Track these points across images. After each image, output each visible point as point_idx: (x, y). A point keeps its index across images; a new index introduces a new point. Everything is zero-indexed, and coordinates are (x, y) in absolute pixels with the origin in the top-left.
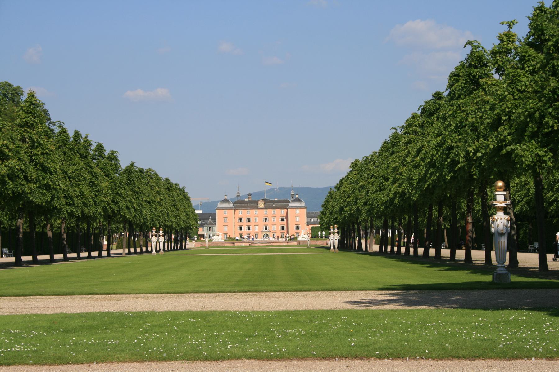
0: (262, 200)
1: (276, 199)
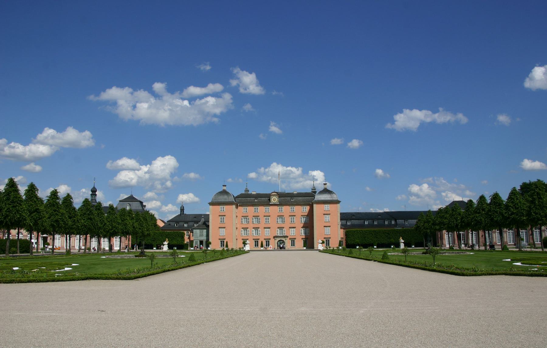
1: (295, 193)
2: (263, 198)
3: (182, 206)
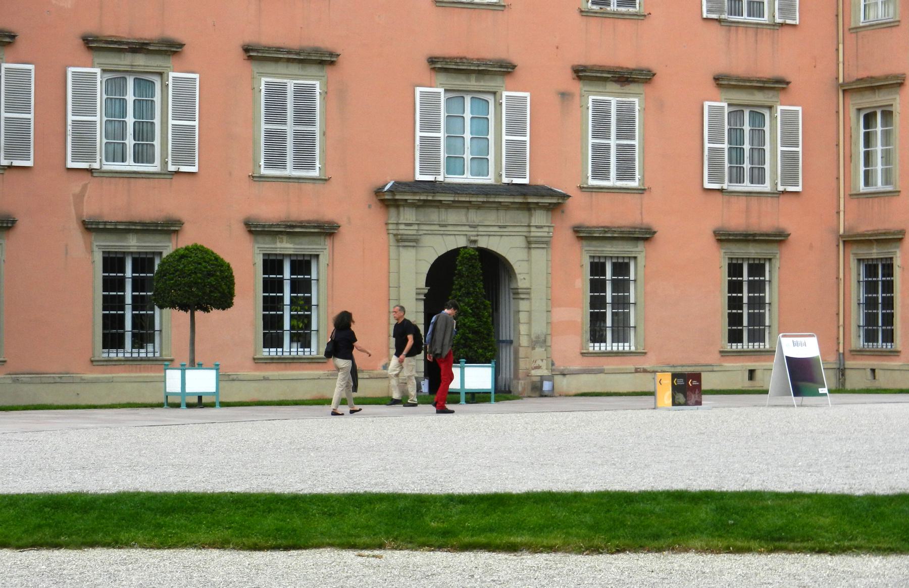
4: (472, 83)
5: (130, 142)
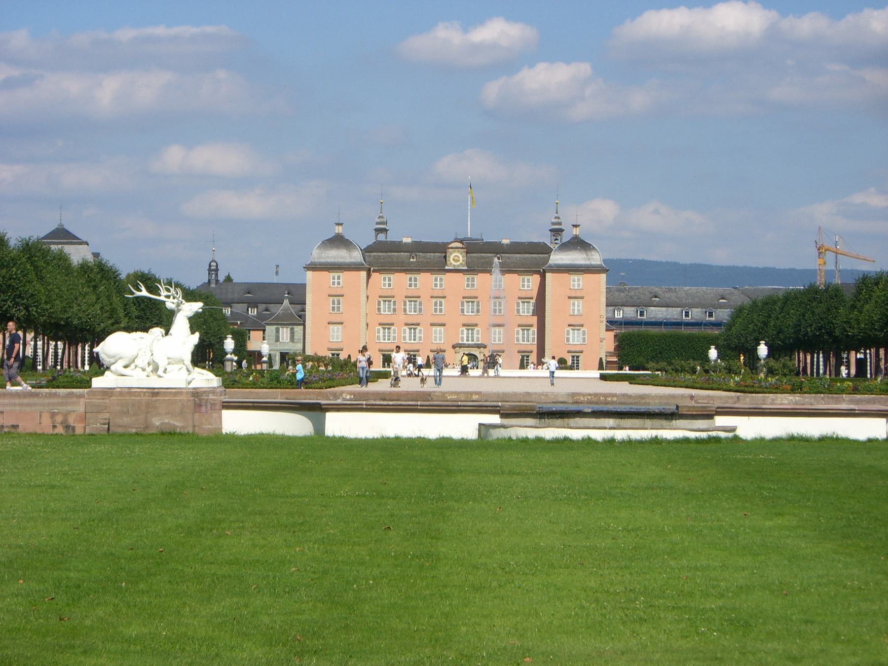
0: (461, 241)
1: (506, 241)
2: (429, 254)
3: (214, 261)
4: (470, 327)
5: (412, 338)
